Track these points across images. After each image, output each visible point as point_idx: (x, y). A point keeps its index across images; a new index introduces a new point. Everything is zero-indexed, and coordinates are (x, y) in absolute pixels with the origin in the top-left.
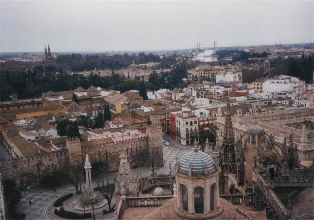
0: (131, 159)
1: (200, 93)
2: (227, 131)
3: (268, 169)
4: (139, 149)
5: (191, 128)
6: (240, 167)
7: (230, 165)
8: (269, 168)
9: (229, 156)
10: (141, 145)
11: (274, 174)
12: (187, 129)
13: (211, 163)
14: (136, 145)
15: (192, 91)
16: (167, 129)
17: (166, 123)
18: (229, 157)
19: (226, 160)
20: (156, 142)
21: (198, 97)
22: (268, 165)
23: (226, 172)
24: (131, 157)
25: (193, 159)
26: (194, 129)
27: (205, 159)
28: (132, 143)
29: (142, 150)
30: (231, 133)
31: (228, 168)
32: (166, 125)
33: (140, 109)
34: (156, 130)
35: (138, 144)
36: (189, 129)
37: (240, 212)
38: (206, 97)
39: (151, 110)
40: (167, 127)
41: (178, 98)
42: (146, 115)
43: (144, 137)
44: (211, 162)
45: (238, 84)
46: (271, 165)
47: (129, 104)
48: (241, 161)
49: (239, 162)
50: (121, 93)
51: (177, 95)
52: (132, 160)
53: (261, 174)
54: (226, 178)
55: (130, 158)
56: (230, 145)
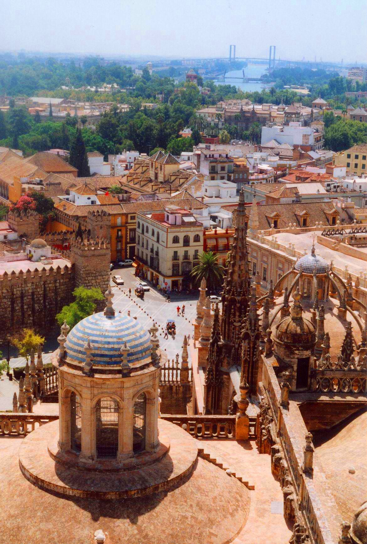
0: (31, 318)
1: (219, 166)
2: (234, 265)
3: (297, 360)
4: (51, 295)
5: (186, 252)
6: (249, 351)
7: (237, 346)
8: (298, 358)
9: (235, 324)
10: (56, 287)
11: (309, 373)
12: (176, 253)
13: (145, 342)
14: (44, 284)
15: (199, 162)
16: (128, 251)
17: (126, 236)
18: (235, 327)
19: (228, 334)
20: (93, 281)
21: (213, 179)
22: (297, 352)
23: (226, 361)
24: (30, 313)
25: (98, 333)
26: (191, 253)
27: (126, 332)
28: (34, 280)
29: (59, 299)
30: (244, 272)
31: (231, 351)
32: (128, 240)
33: (67, 197)
34: (96, 253)
35: (48, 282)
36: (181, 254)
37: (206, 457)
38: (232, 178)
39: (93, 202)
40: (128, 245)
41: (163, 176)
42: (79, 214)
43: (66, 267)
44: (141, 340)
45: (311, 153)
46: (302, 350)
47: (40, 183)
48: (252, 339)
49: (247, 341)
50: (26, 155)
51: (161, 170)
52: (33, 320)
53: (278, 371)
54: (225, 376)
55: (29, 315)
56: (240, 298)
